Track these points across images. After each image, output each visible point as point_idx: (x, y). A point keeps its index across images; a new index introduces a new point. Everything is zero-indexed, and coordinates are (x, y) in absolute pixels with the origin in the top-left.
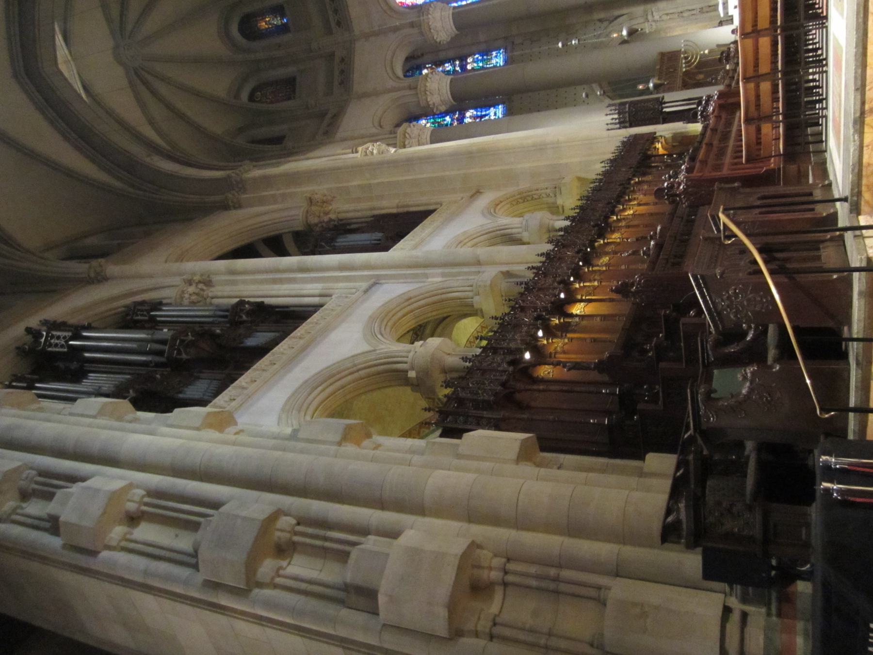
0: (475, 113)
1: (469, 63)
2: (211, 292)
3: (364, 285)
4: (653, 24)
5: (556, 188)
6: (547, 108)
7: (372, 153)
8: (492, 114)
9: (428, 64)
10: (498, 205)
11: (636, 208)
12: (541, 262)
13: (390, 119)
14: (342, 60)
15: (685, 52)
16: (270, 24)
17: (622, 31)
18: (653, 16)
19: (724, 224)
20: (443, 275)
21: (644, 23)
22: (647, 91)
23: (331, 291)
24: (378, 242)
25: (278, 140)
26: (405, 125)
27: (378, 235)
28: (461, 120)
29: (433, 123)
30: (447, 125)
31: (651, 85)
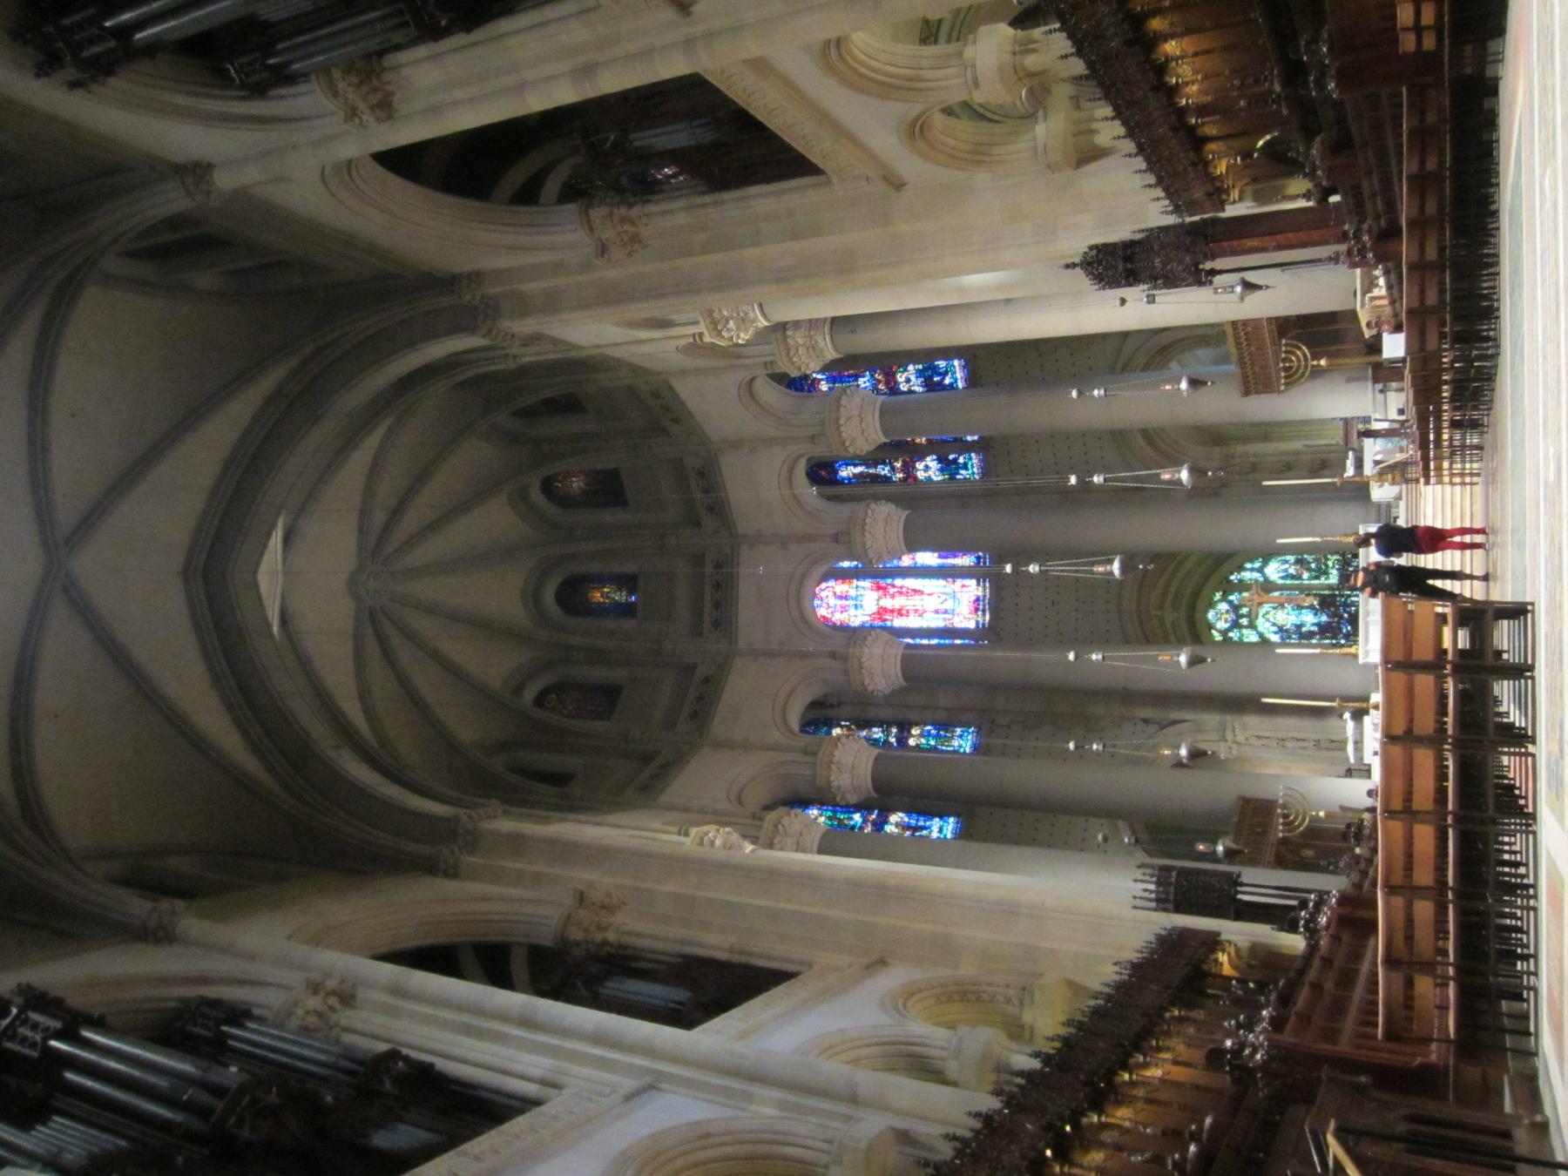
0: (906, 819)
1: (914, 736)
2: (346, 1017)
3: (630, 1084)
4: (1235, 747)
5: (1024, 989)
6: (1033, 842)
7: (712, 843)
8: (935, 829)
9: (845, 721)
10: (913, 994)
11: (1169, 1067)
12: (972, 1130)
13: (758, 795)
14: (706, 681)
15: (1284, 806)
16: (608, 598)
17: (1179, 747)
18: (1235, 736)
19: (1336, 1160)
20: (782, 1105)
21: (1220, 741)
22: (1211, 857)
23: (564, 1080)
24: (680, 1007)
25: (560, 779)
26: (781, 810)
27: (680, 994)
28: (879, 825)
29: (830, 818)
30: (853, 828)
31: (1220, 848)
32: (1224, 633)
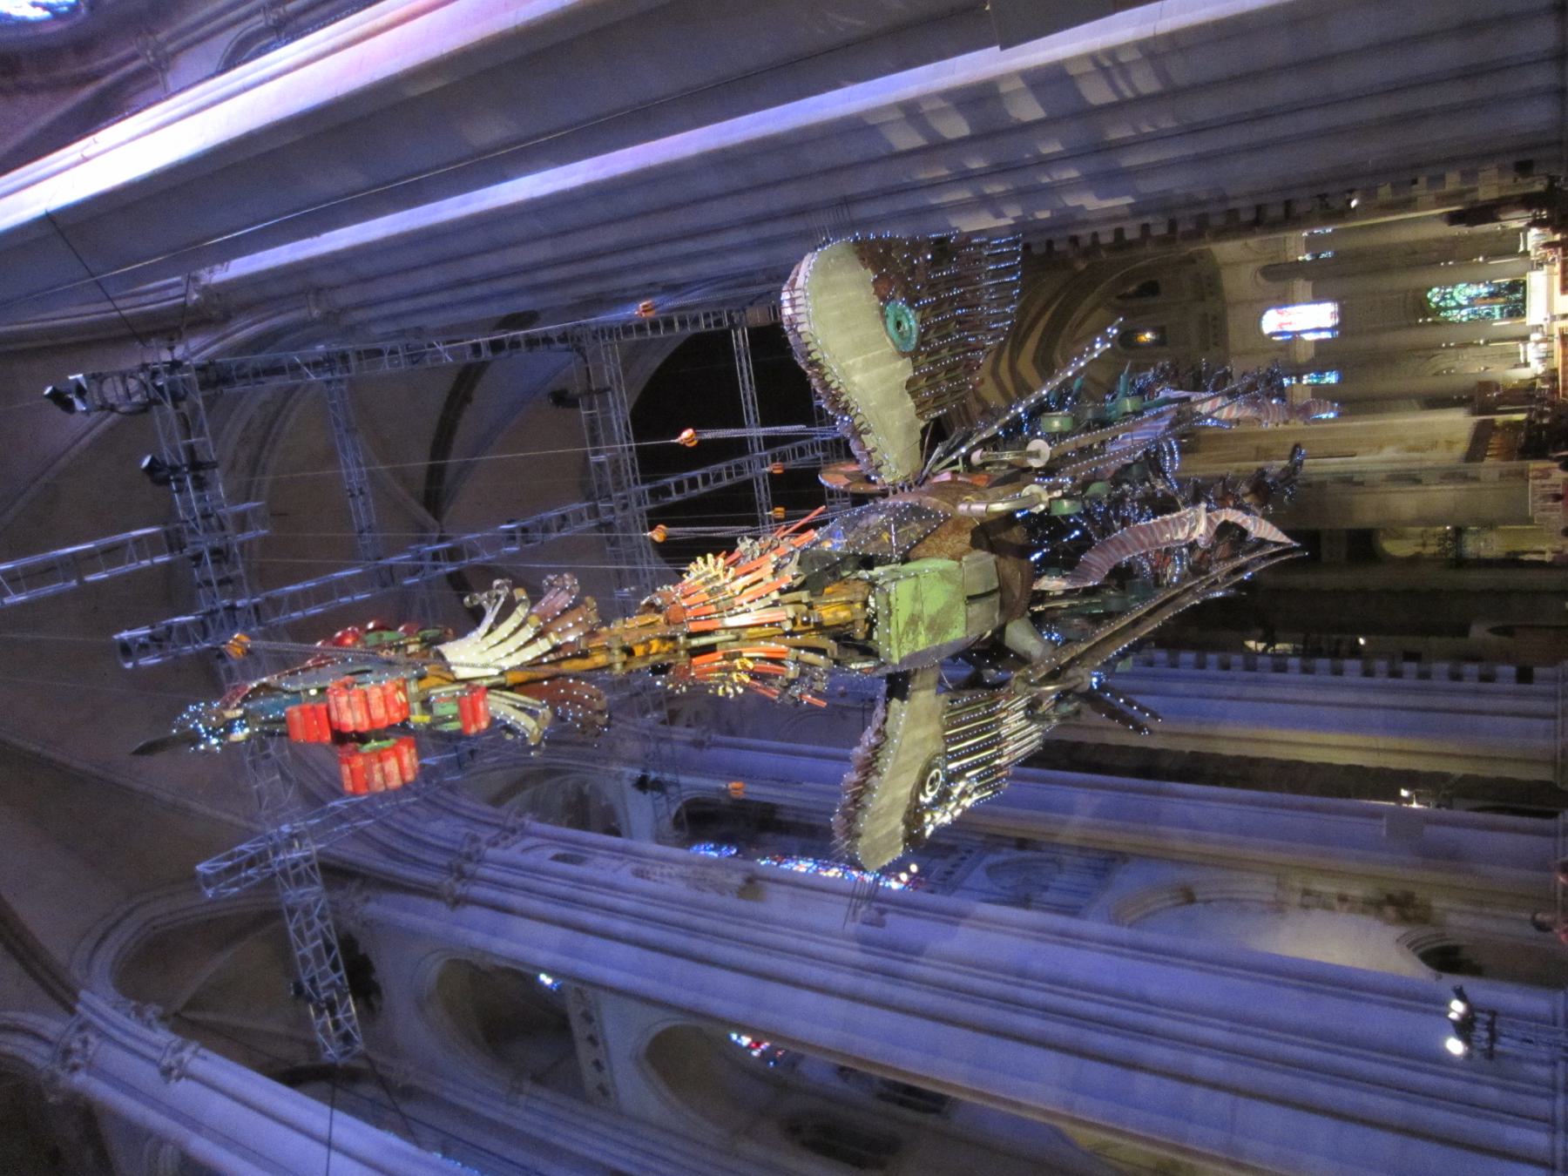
32: (1437, 303)
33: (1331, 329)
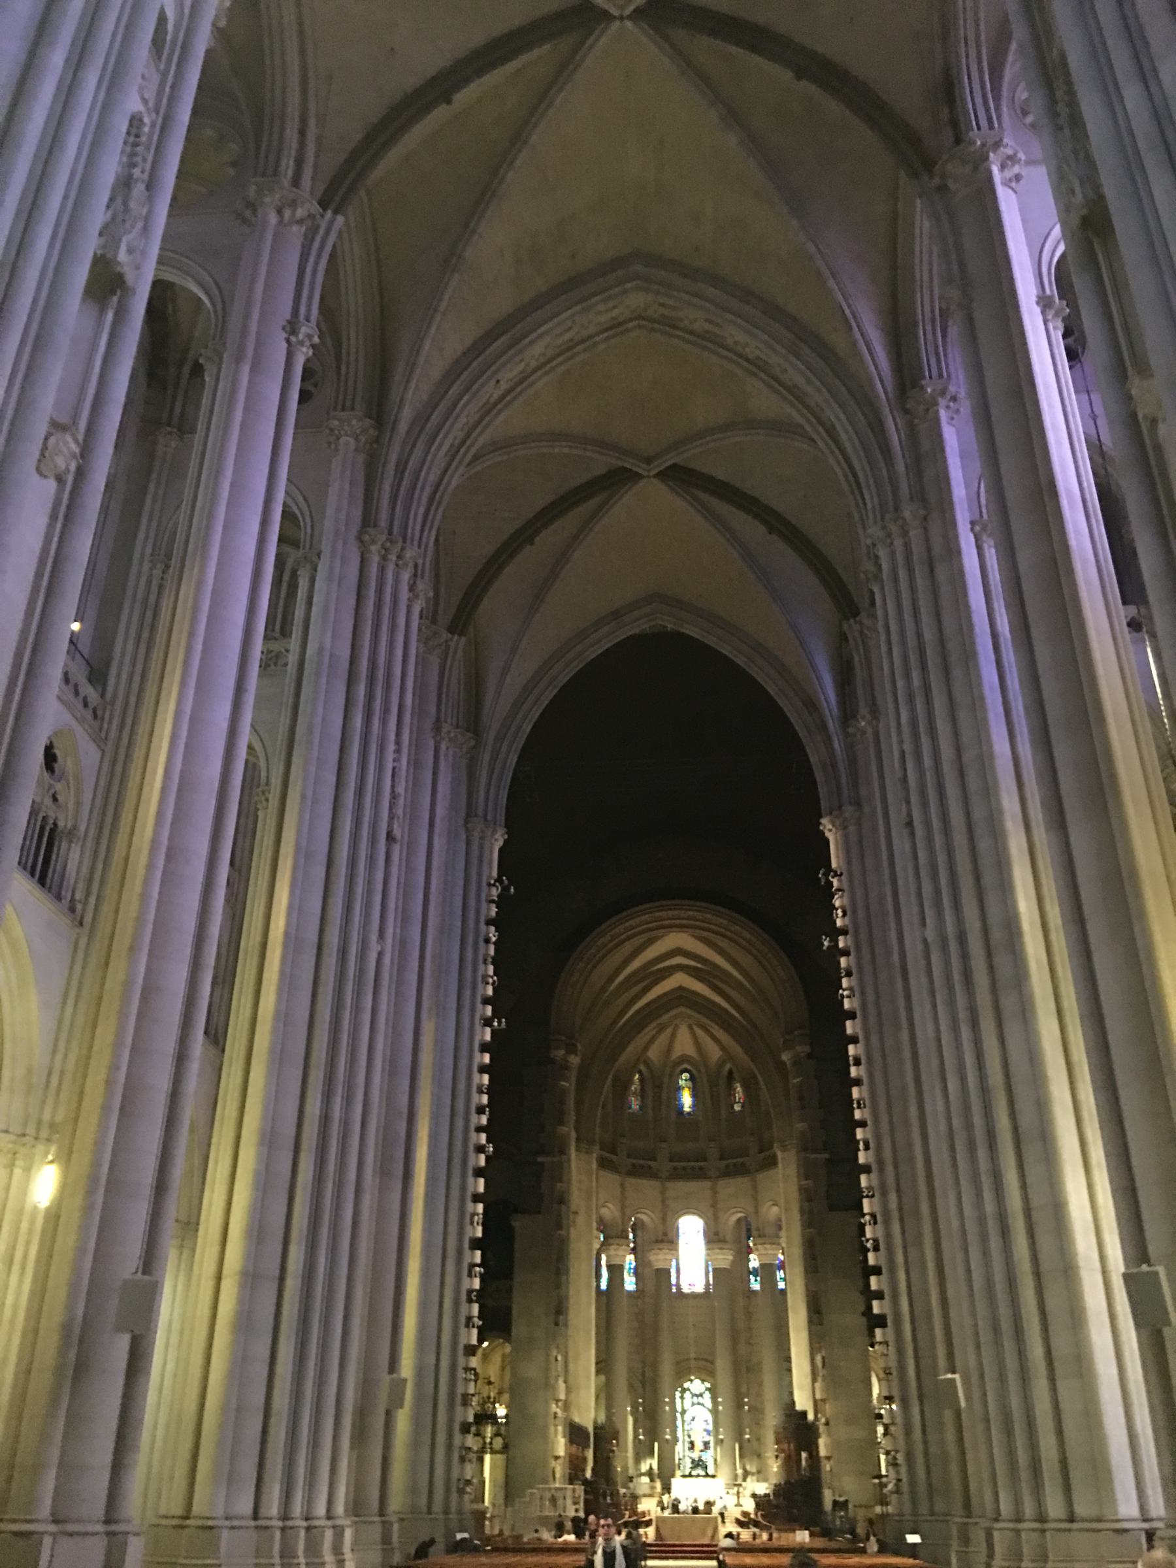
14: (650, 1167)
33: (678, 1285)
